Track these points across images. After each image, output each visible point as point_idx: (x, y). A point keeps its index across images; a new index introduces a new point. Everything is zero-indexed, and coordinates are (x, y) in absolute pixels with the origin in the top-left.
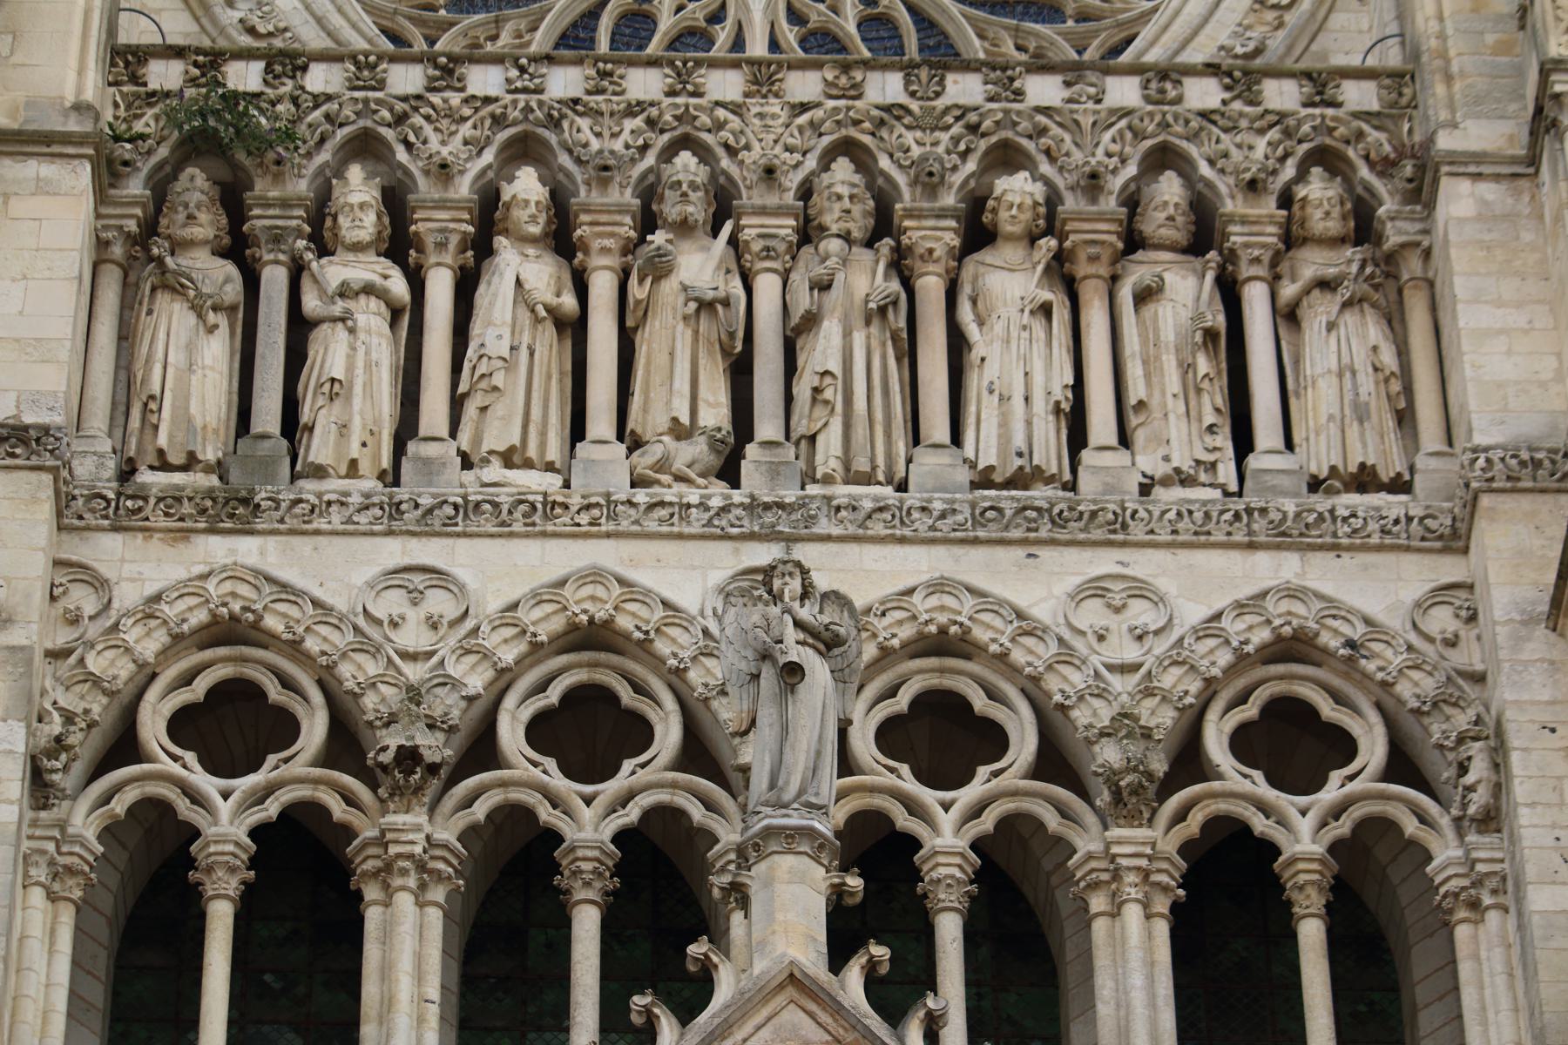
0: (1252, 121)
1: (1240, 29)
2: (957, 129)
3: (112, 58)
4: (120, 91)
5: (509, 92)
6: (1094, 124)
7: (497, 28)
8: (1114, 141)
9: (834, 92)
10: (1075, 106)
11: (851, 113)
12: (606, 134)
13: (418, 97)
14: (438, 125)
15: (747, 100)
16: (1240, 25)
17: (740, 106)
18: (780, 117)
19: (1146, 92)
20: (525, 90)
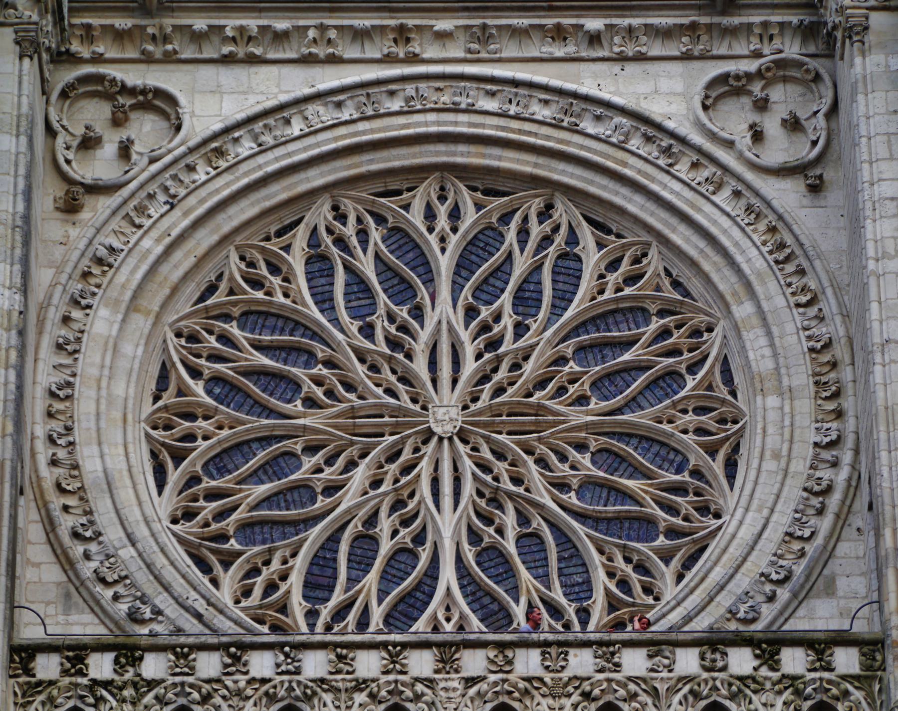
0: (774, 684)
1: (775, 558)
2: (576, 698)
3: (11, 656)
4: (17, 683)
5: (278, 674)
6: (668, 689)
7: (270, 555)
8: (681, 703)
9: (494, 668)
10: (655, 675)
11: (506, 686)
12: (343, 706)
13: (218, 681)
14: (230, 702)
15: (437, 676)
16: (775, 555)
17: (431, 681)
18: (458, 689)
19: (703, 663)
20: (288, 672)
